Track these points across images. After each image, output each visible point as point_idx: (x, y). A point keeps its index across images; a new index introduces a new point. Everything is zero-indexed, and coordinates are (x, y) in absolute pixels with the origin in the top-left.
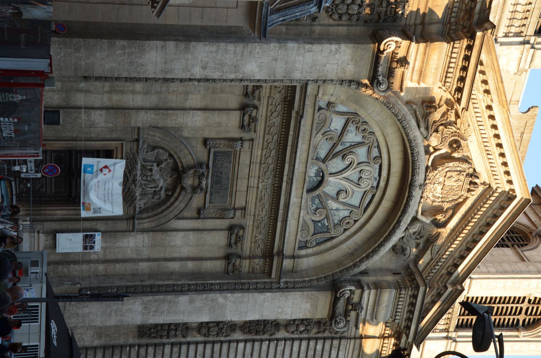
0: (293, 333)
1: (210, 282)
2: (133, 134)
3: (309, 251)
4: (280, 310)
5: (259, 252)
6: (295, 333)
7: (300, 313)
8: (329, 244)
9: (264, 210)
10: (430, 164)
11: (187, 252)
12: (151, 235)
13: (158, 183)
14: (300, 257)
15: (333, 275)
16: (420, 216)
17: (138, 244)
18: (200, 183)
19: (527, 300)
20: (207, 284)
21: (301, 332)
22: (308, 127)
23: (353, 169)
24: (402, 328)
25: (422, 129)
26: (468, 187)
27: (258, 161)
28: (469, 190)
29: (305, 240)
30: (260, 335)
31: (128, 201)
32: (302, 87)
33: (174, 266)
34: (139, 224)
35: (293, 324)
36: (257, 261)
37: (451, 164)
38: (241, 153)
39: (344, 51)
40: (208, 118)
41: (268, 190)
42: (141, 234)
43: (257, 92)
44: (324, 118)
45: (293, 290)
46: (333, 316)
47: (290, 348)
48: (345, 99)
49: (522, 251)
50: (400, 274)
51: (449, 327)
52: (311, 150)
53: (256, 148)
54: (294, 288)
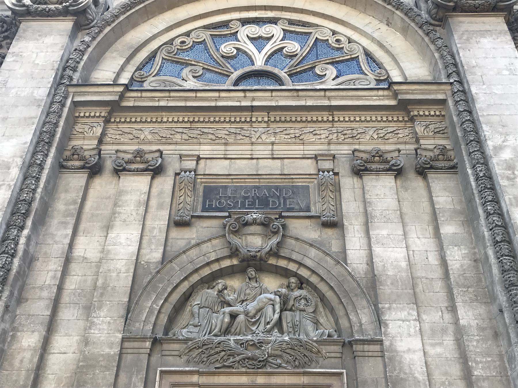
1: (473, 184)
2: (142, 351)
9: (318, 132)
11: (423, 240)
12: (387, 306)
13: (264, 300)
17: (412, 330)
18: (254, 222)
20: (478, 186)
23: (246, 44)
33: (457, 257)
34: (361, 331)
38: (206, 173)
40: (125, 221)
42: (386, 325)
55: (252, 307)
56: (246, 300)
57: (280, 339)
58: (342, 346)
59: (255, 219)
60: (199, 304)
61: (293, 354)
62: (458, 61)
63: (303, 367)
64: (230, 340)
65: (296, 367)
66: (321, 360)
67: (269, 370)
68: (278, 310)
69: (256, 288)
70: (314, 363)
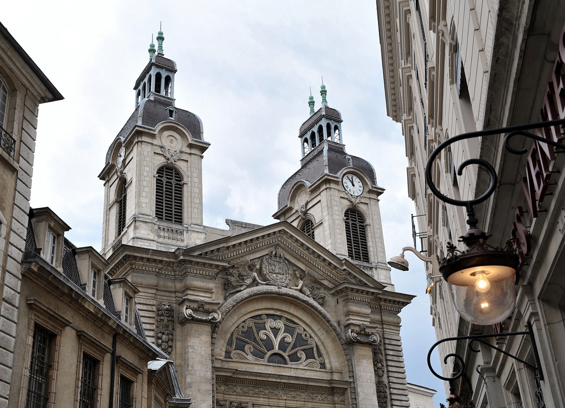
0: (383, 372)
3: (327, 361)
4: (369, 381)
5: (330, 398)
6: (383, 370)
7: (370, 367)
8: (321, 348)
9: (301, 394)
10: (265, 283)
14: (331, 368)
15: (342, 345)
16: (299, 288)
19: (347, 221)
21: (382, 366)
22: (243, 365)
24: (373, 297)
25: (242, 289)
26: (278, 258)
27: (267, 400)
28: (280, 257)
29: (319, 364)
30: (387, 395)
32: (216, 371)
35: (377, 371)
36: (336, 399)
37: (264, 269)
39: (192, 343)
41: (287, 392)
43: (221, 403)
44: (237, 354)
45: (354, 372)
46: (370, 344)
47: (394, 373)
48: (224, 341)
49: (316, 224)
50: (337, 299)
51: (369, 267)
52: (259, 363)
53: (258, 402)
54: (353, 372)
62: (354, 370)
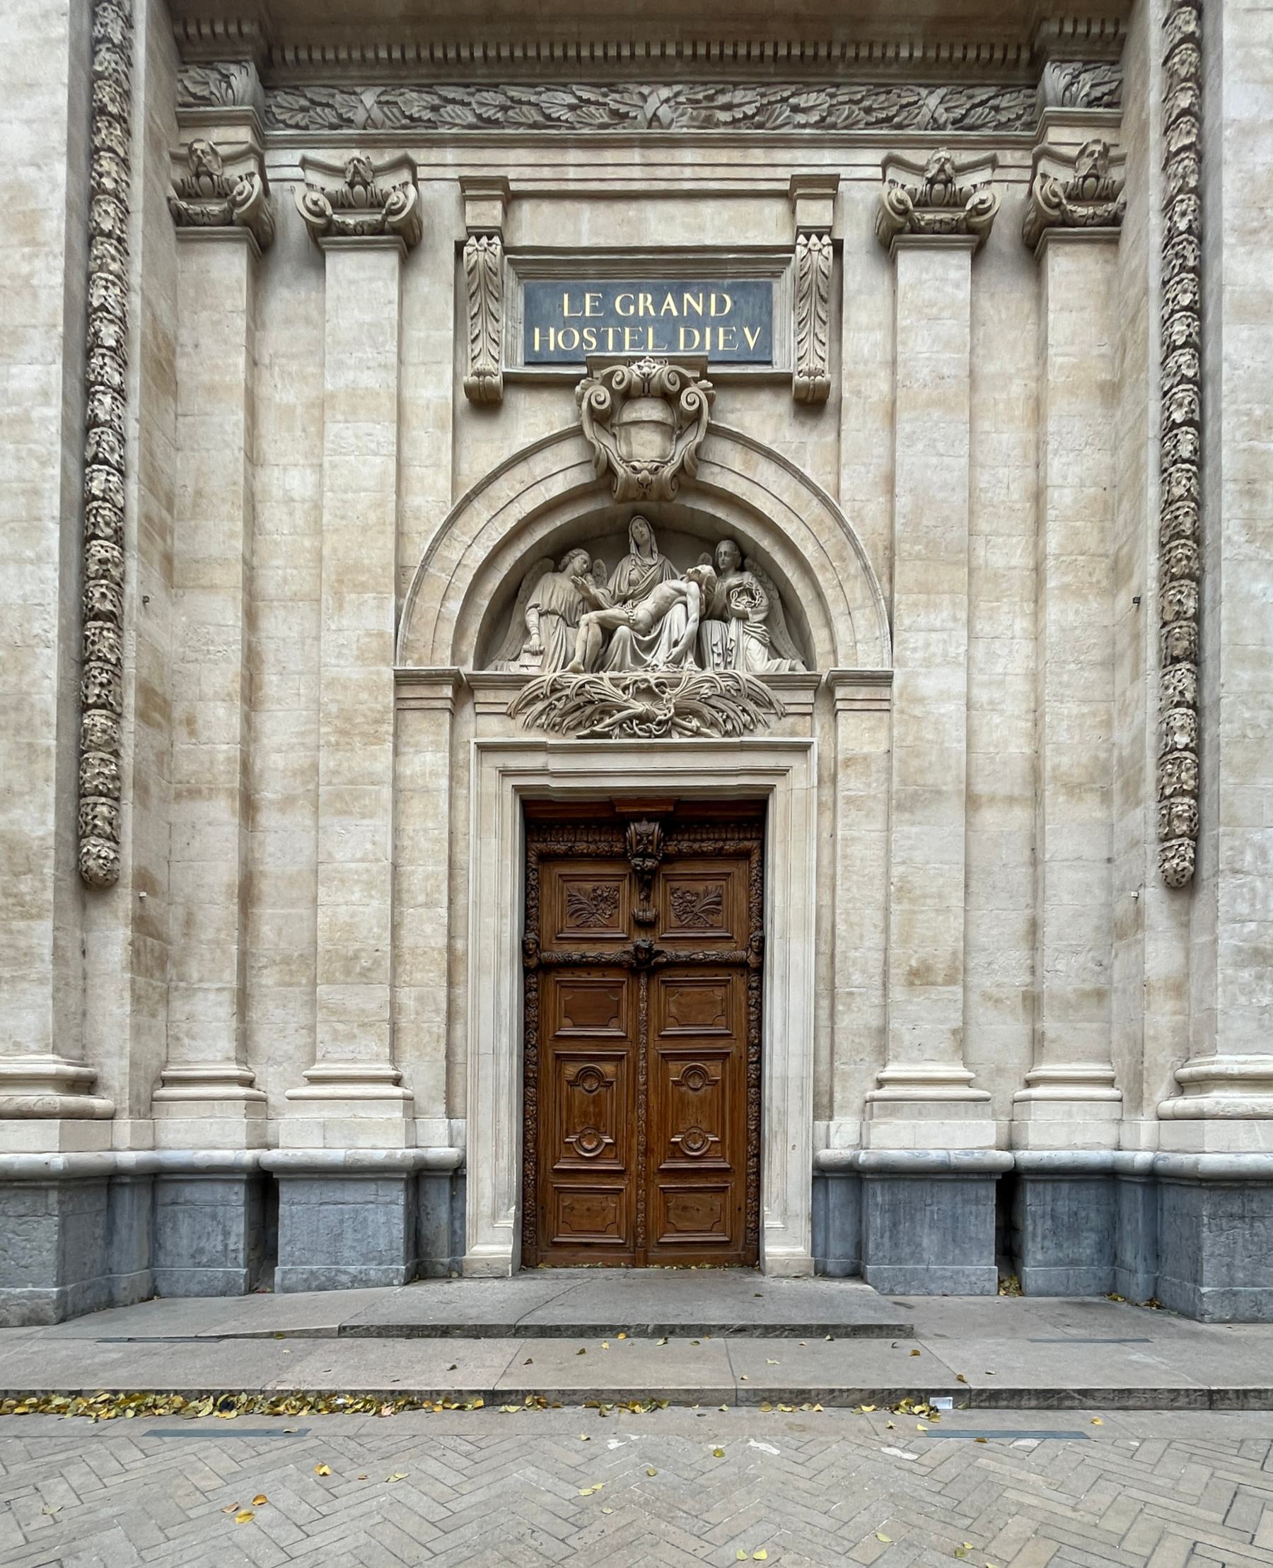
31: (744, 710)
55: (643, 610)
56: (632, 597)
57: (698, 676)
58: (816, 691)
59: (647, 378)
60: (536, 606)
61: (723, 707)
63: (741, 734)
64: (601, 679)
65: (727, 734)
66: (774, 718)
67: (676, 739)
68: (694, 615)
69: (651, 566)
70: (760, 726)
